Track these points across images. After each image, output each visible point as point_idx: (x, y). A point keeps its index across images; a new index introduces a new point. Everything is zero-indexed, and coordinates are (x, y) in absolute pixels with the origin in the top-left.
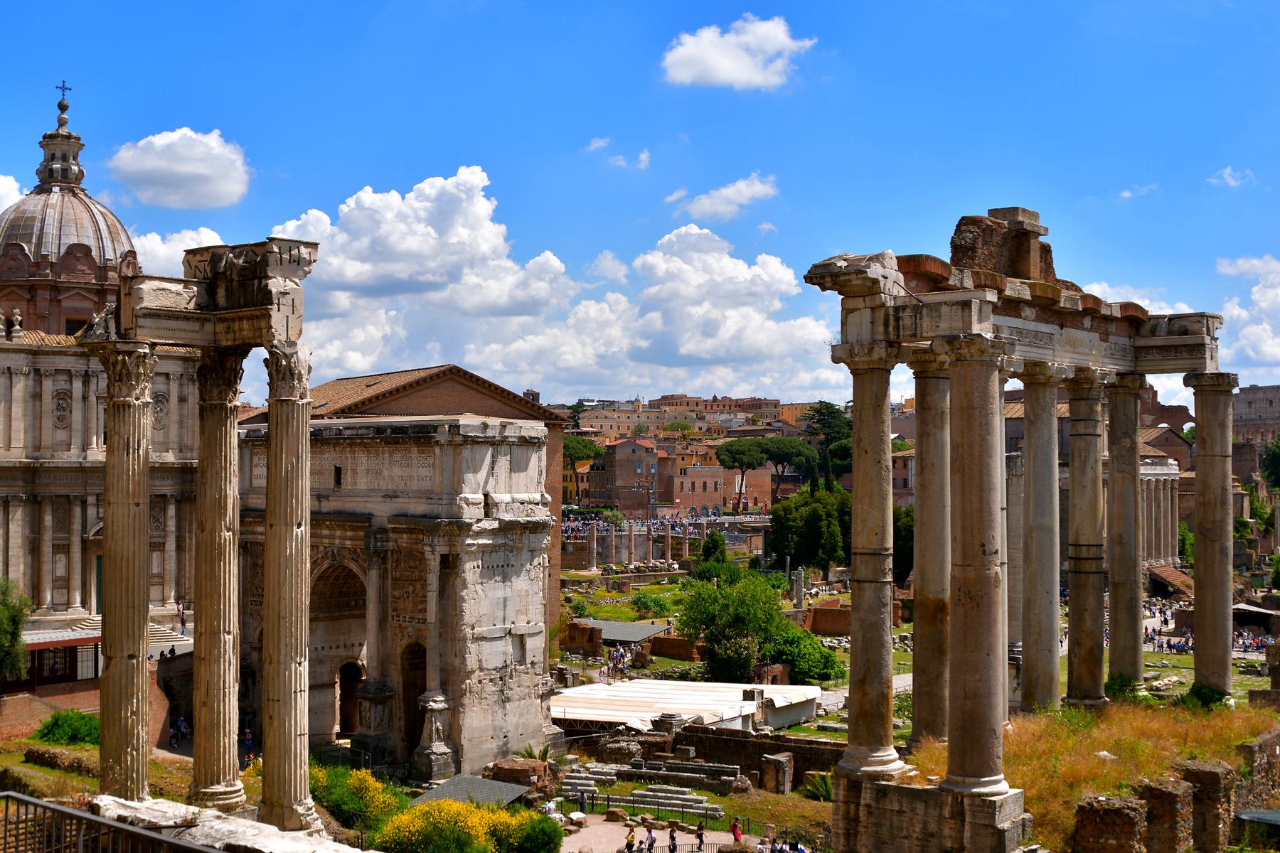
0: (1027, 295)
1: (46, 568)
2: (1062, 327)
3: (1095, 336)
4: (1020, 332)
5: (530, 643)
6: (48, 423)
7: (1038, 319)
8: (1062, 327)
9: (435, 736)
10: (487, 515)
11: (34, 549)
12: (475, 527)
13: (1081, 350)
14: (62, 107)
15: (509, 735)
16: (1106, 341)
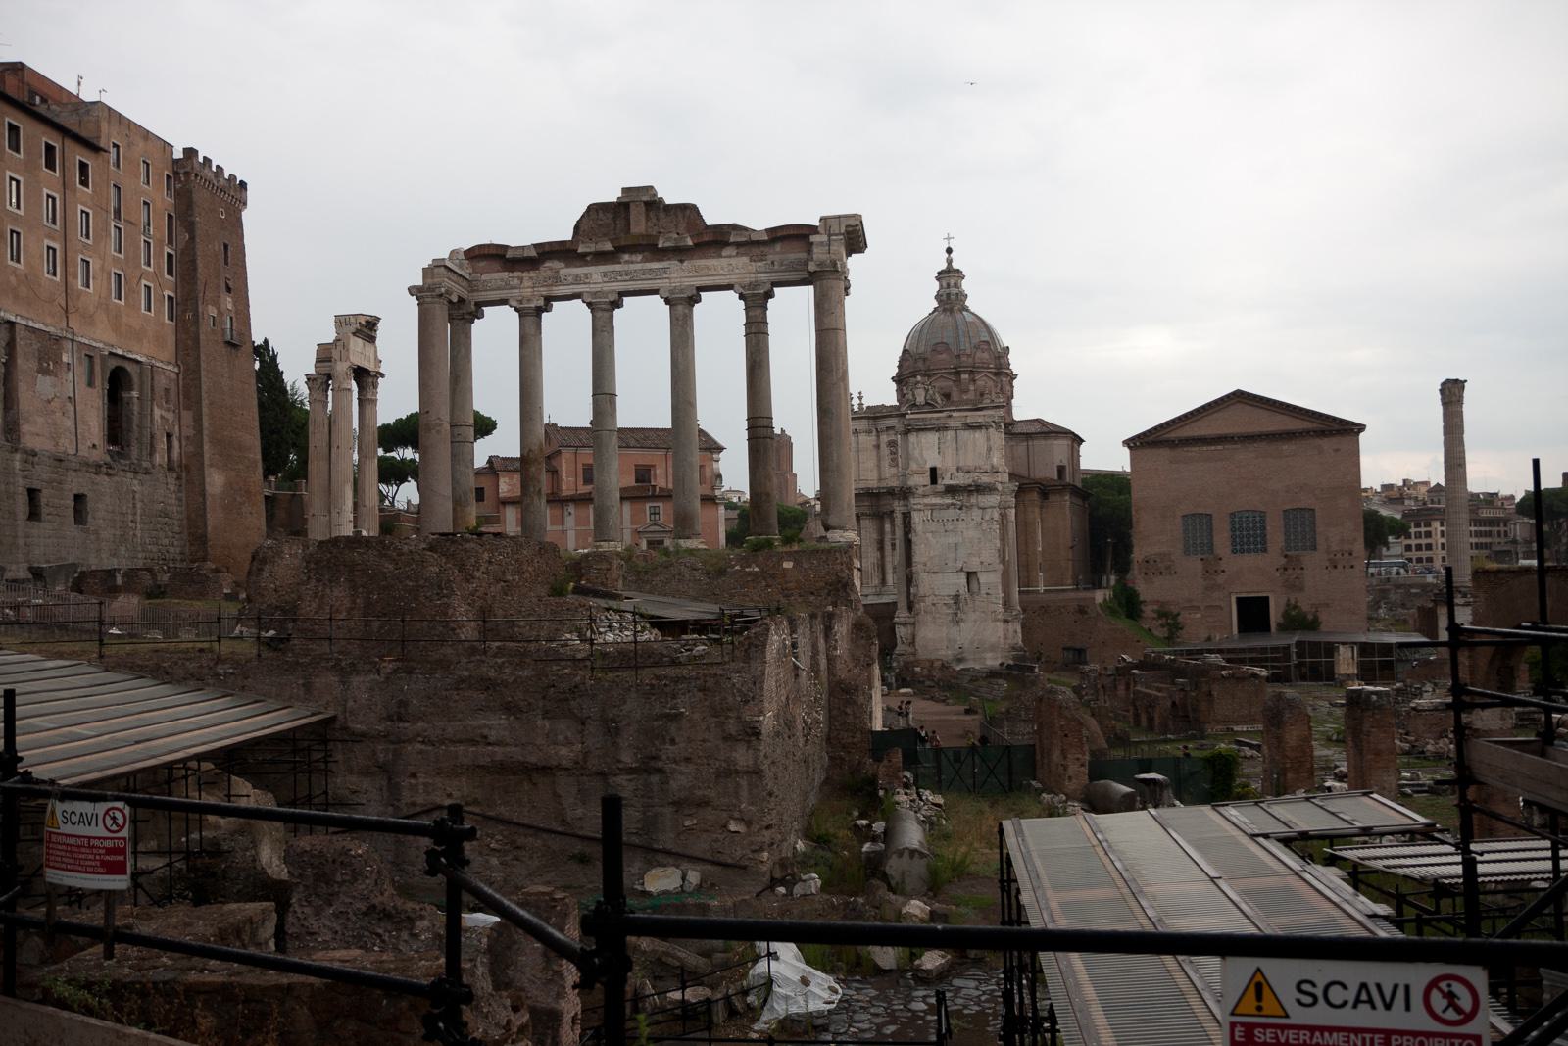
0: (608, 247)
1: (888, 559)
2: (682, 261)
3: (745, 259)
4: (620, 273)
5: (983, 578)
6: (886, 463)
7: (645, 260)
8: (682, 261)
9: (899, 641)
10: (934, 480)
11: (881, 549)
12: (921, 491)
13: (711, 273)
14: (949, 251)
15: (966, 646)
16: (762, 260)
